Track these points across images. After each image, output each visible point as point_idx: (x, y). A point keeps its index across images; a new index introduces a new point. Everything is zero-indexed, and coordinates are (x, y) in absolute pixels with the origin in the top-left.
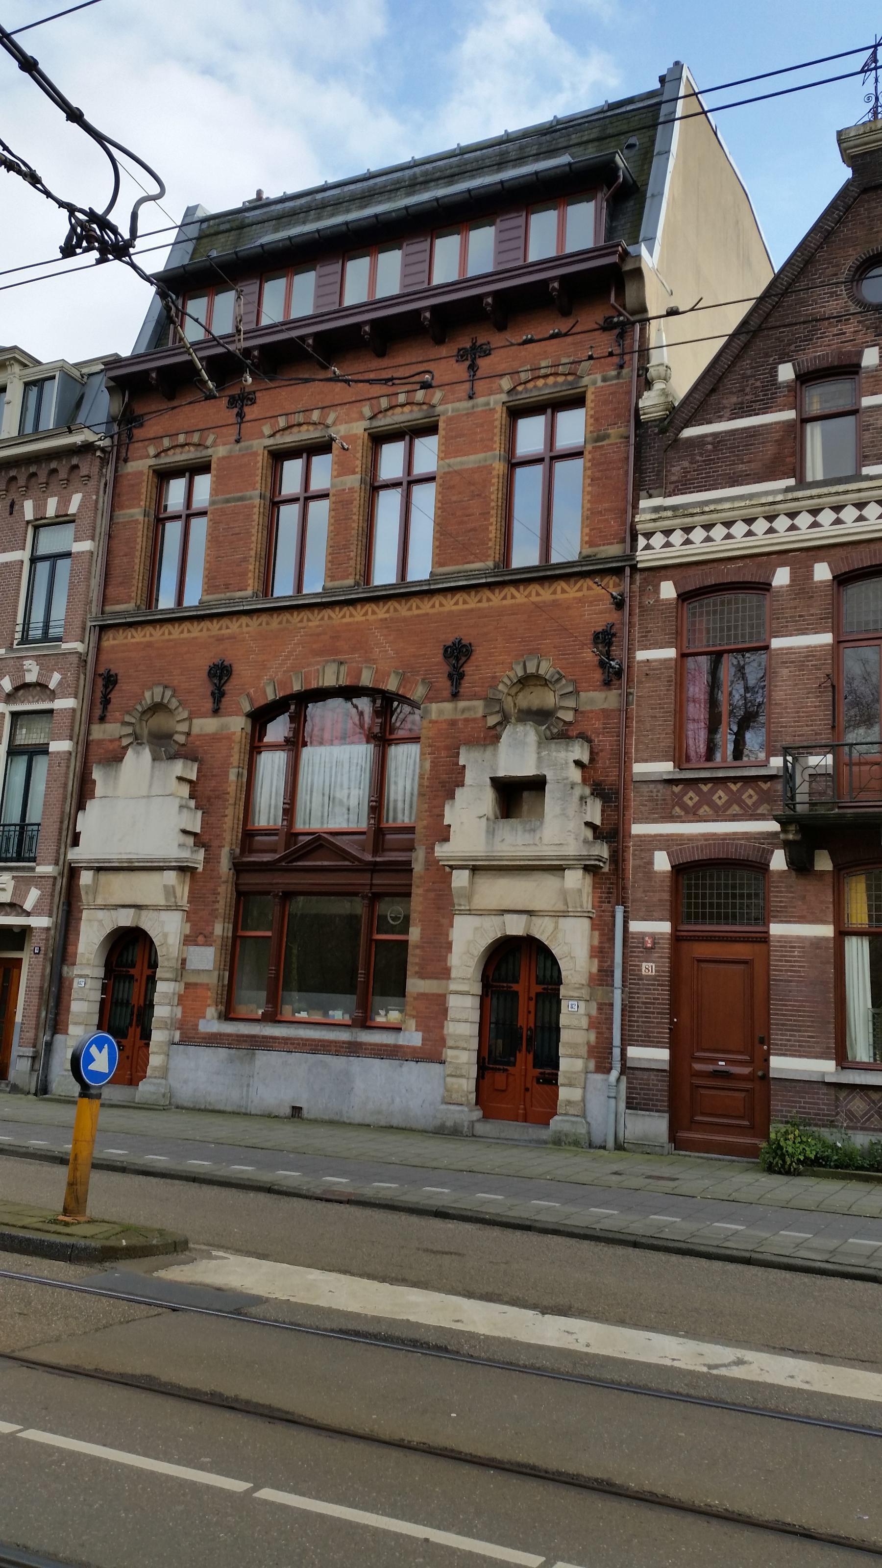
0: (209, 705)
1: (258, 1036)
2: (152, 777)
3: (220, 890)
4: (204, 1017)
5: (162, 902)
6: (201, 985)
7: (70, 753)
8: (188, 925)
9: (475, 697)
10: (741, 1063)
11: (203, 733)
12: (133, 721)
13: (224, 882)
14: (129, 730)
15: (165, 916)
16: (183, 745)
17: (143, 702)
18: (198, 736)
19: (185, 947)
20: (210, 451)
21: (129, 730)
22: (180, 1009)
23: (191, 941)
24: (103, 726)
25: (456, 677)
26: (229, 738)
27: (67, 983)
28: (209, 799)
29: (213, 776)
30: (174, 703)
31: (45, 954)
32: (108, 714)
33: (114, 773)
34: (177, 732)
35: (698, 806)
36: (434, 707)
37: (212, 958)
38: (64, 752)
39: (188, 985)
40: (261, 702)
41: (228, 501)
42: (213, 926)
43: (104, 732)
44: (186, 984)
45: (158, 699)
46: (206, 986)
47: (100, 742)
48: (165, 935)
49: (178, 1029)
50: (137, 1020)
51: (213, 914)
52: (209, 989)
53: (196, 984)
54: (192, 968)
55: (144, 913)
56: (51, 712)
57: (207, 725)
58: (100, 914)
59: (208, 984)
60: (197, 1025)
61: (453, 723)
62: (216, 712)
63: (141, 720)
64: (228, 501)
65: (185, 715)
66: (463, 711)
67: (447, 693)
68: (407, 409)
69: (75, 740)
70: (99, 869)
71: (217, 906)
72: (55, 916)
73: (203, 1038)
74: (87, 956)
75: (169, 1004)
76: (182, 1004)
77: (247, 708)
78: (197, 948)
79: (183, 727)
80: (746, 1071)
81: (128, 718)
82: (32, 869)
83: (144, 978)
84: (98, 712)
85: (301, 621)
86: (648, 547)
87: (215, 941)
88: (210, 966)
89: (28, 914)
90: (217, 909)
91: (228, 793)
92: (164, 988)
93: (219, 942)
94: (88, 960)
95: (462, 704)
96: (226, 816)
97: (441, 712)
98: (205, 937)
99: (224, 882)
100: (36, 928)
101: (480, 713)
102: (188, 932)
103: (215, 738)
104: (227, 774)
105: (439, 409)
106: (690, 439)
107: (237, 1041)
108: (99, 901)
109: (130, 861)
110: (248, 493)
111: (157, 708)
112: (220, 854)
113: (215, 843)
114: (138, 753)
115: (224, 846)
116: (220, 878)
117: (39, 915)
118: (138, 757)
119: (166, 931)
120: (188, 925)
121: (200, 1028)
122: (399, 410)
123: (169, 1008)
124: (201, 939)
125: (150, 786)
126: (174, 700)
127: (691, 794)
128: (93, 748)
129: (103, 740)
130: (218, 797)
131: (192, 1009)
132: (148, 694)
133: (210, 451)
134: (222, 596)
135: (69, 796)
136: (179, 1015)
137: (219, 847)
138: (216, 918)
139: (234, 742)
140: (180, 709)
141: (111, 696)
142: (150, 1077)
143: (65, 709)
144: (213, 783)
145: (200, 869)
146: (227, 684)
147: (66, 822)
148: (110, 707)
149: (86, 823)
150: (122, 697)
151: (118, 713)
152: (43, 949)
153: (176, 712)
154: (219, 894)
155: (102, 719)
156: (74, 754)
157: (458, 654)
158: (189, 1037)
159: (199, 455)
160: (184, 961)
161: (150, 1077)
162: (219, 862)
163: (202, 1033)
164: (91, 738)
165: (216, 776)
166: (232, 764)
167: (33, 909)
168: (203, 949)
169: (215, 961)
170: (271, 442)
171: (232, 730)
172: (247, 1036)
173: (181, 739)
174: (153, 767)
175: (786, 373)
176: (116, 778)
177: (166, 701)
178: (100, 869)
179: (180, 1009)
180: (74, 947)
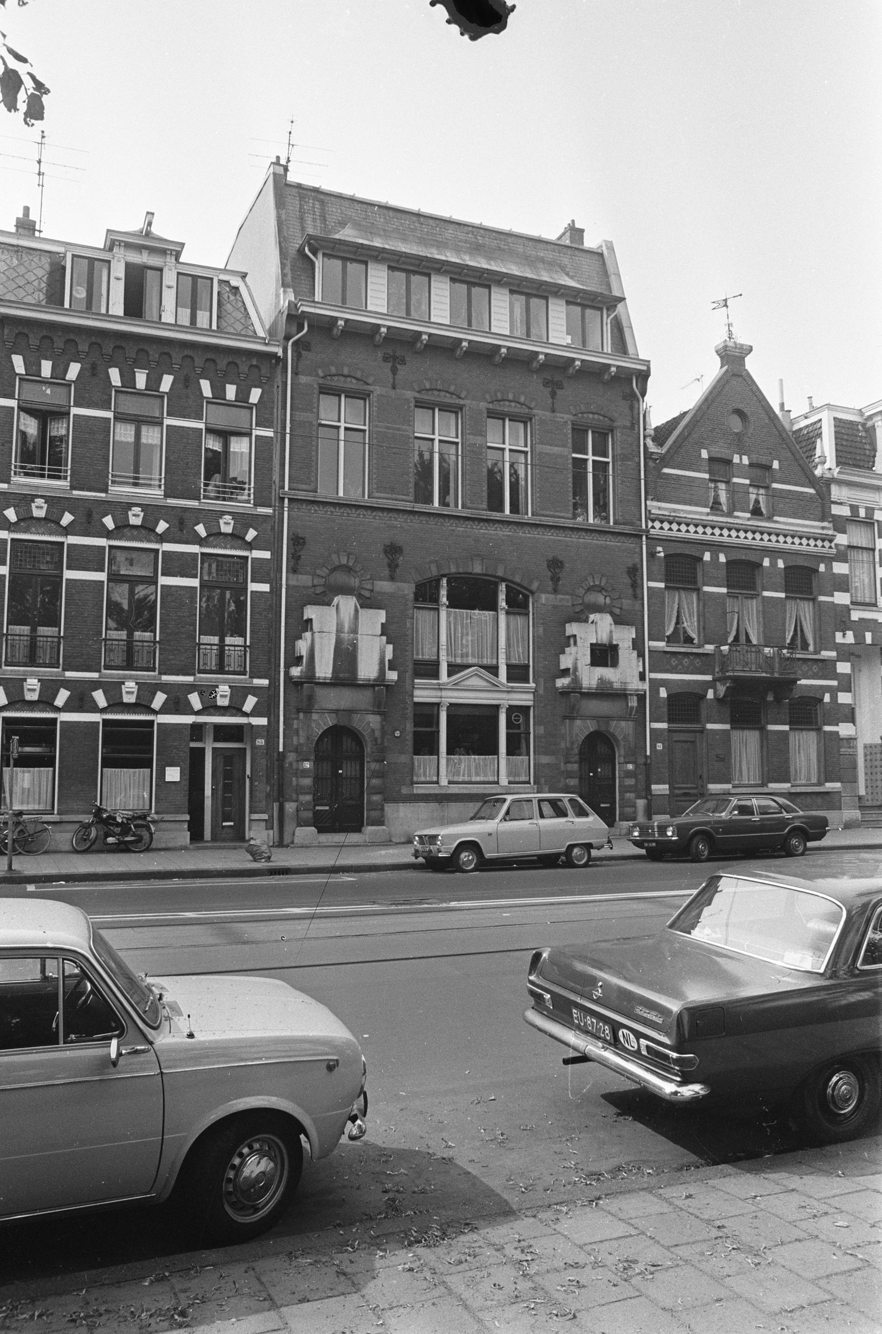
0: (386, 572)
9: (567, 594)
10: (692, 788)
20: (371, 388)
21: (322, 581)
24: (295, 576)
25: (555, 579)
34: (364, 589)
35: (677, 666)
36: (543, 596)
41: (388, 428)
61: (555, 607)
62: (392, 578)
64: (388, 428)
66: (561, 600)
67: (550, 589)
68: (513, 404)
77: (419, 578)
79: (369, 587)
80: (695, 791)
81: (318, 572)
85: (451, 526)
86: (653, 527)
95: (559, 597)
97: (547, 599)
101: (570, 604)
105: (535, 411)
106: (665, 474)
110: (404, 427)
122: (507, 403)
127: (674, 659)
133: (371, 388)
134: (390, 496)
141: (301, 553)
157: (555, 565)
159: (362, 387)
170: (417, 395)
175: (704, 454)
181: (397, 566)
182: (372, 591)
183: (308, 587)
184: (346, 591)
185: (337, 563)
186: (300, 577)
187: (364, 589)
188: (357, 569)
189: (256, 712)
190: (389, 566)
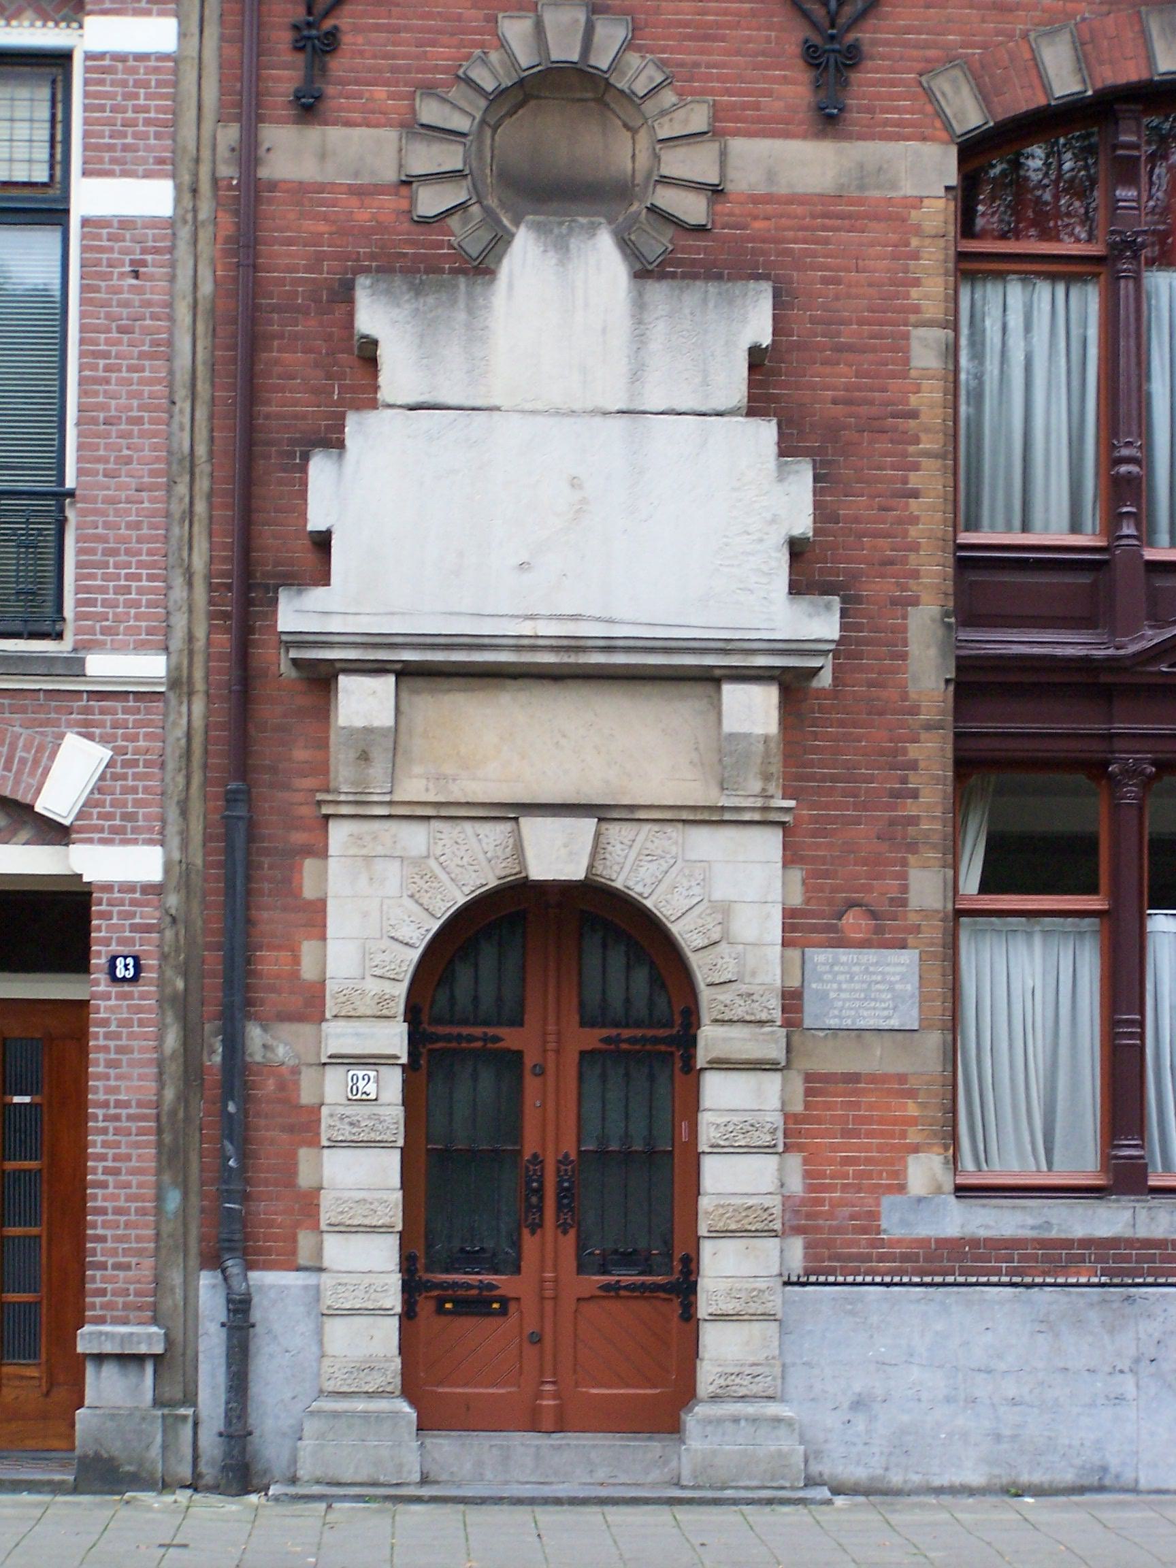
0: (795, 89)
1: (1130, 1243)
2: (639, 338)
3: (913, 751)
4: (902, 1188)
5: (695, 790)
6: (873, 1078)
7: (171, 223)
8: (797, 875)
11: (782, 189)
12: (460, 123)
13: (929, 727)
14: (450, 157)
15: (706, 844)
16: (700, 229)
17: (494, 57)
18: (755, 199)
19: (795, 954)
21: (450, 157)
22: (795, 1161)
23: (814, 929)
24: (314, 134)
26: (895, 216)
27: (271, 1085)
28: (833, 431)
29: (839, 348)
30: (639, 74)
31: (161, 983)
32: (331, 90)
33: (462, 316)
34: (666, 181)
37: (911, 987)
38: (153, 222)
39: (816, 1084)
40: (1022, 99)
42: (904, 876)
43: (323, 156)
44: (809, 1077)
45: (565, 50)
46: (900, 1086)
47: (301, 191)
48: (724, 910)
49: (798, 1230)
50: (560, 1207)
51: (899, 839)
52: (912, 1094)
53: (853, 1078)
54: (833, 1023)
55: (617, 833)
56: (62, 58)
57: (807, 165)
58: (414, 837)
59: (902, 1078)
60: (874, 1216)
62: (829, 119)
63: (483, 122)
65: (697, 118)
69: (186, 178)
70: (405, 673)
71: (911, 808)
72: (175, 842)
73: (905, 1258)
74: (373, 987)
75: (768, 1149)
76: (800, 1148)
77: (970, 115)
78: (845, 955)
79: (697, 164)
81: (430, 112)
82: (74, 667)
83: (571, 1059)
84: (285, 76)
87: (917, 929)
88: (909, 1017)
89: (55, 833)
90: (913, 821)
91: (914, 415)
92: (733, 1102)
93: (934, 932)
94: (382, 1000)
96: (915, 494)
98: (874, 915)
99: (929, 727)
100: (108, 887)
102: (797, 900)
103: (833, 211)
104: (901, 346)
107: (1047, 1259)
108: (414, 788)
109: (575, 645)
111: (572, 86)
112: (904, 629)
113: (877, 588)
114: (561, 246)
115: (915, 602)
116: (914, 711)
117: (118, 835)
118: (561, 263)
119: (717, 896)
120: (797, 875)
121: (884, 1224)
123: (772, 1162)
124: (853, 921)
125: (636, 375)
126: (634, 60)
128: (280, 216)
129: (321, 188)
130: (874, 427)
131: (846, 1161)
132: (516, 30)
135: (182, 393)
136: (796, 1185)
137: (895, 602)
138: (912, 848)
139: (918, 231)
140: (668, 97)
142: (715, 1398)
143: (141, 57)
144: (843, 375)
145: (825, 680)
146: (871, 22)
147: (182, 489)
148: (338, 65)
149: (330, 494)
150: (396, 30)
151: (380, 92)
152: (149, 962)
153: (650, 107)
154: (913, 766)
155: (309, 107)
156: (185, 233)
158: (838, 1250)
160: (792, 1000)
161: (715, 1398)
162: (904, 656)
163: (899, 1242)
164: (264, 173)
165: (850, 348)
166: (917, 310)
167: (80, 815)
168: (870, 956)
169: (924, 999)
171: (908, 189)
172: (1086, 1243)
173: (693, 208)
174: (639, 305)
176: (476, 333)
177: (602, 60)
178: (431, 670)
179: (795, 1161)
180: (284, 955)
181: (852, 57)
182: (716, 192)
183: (378, 189)
184: (561, 196)
185: (525, 58)
186: (335, 134)
187: (666, 181)
188: (641, 88)
189: (103, 818)
190: (812, 56)
